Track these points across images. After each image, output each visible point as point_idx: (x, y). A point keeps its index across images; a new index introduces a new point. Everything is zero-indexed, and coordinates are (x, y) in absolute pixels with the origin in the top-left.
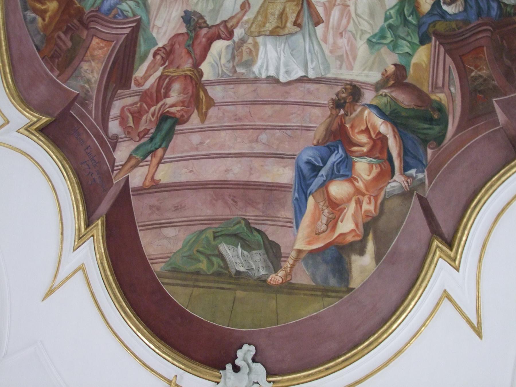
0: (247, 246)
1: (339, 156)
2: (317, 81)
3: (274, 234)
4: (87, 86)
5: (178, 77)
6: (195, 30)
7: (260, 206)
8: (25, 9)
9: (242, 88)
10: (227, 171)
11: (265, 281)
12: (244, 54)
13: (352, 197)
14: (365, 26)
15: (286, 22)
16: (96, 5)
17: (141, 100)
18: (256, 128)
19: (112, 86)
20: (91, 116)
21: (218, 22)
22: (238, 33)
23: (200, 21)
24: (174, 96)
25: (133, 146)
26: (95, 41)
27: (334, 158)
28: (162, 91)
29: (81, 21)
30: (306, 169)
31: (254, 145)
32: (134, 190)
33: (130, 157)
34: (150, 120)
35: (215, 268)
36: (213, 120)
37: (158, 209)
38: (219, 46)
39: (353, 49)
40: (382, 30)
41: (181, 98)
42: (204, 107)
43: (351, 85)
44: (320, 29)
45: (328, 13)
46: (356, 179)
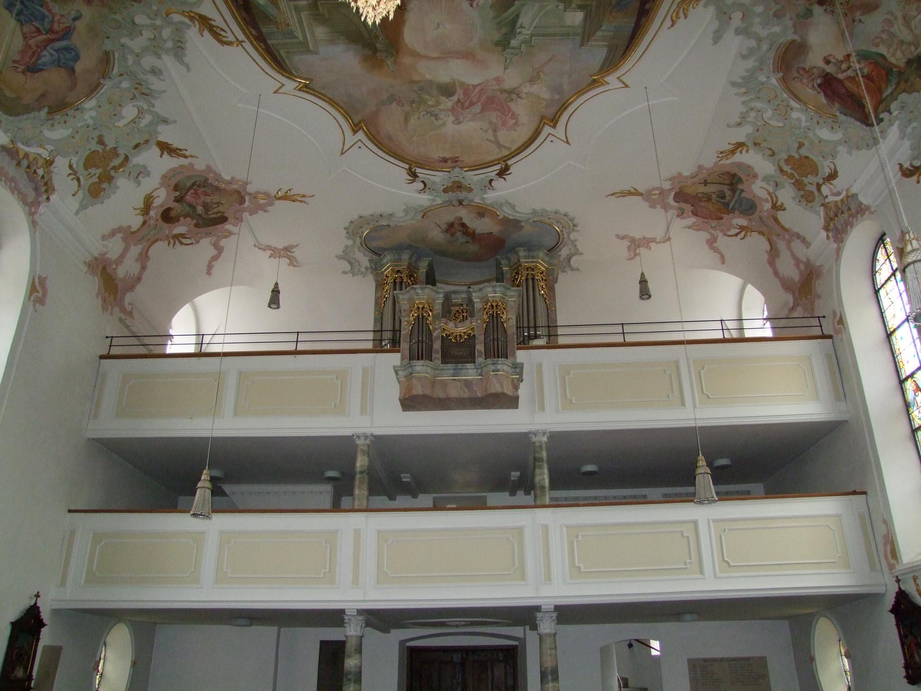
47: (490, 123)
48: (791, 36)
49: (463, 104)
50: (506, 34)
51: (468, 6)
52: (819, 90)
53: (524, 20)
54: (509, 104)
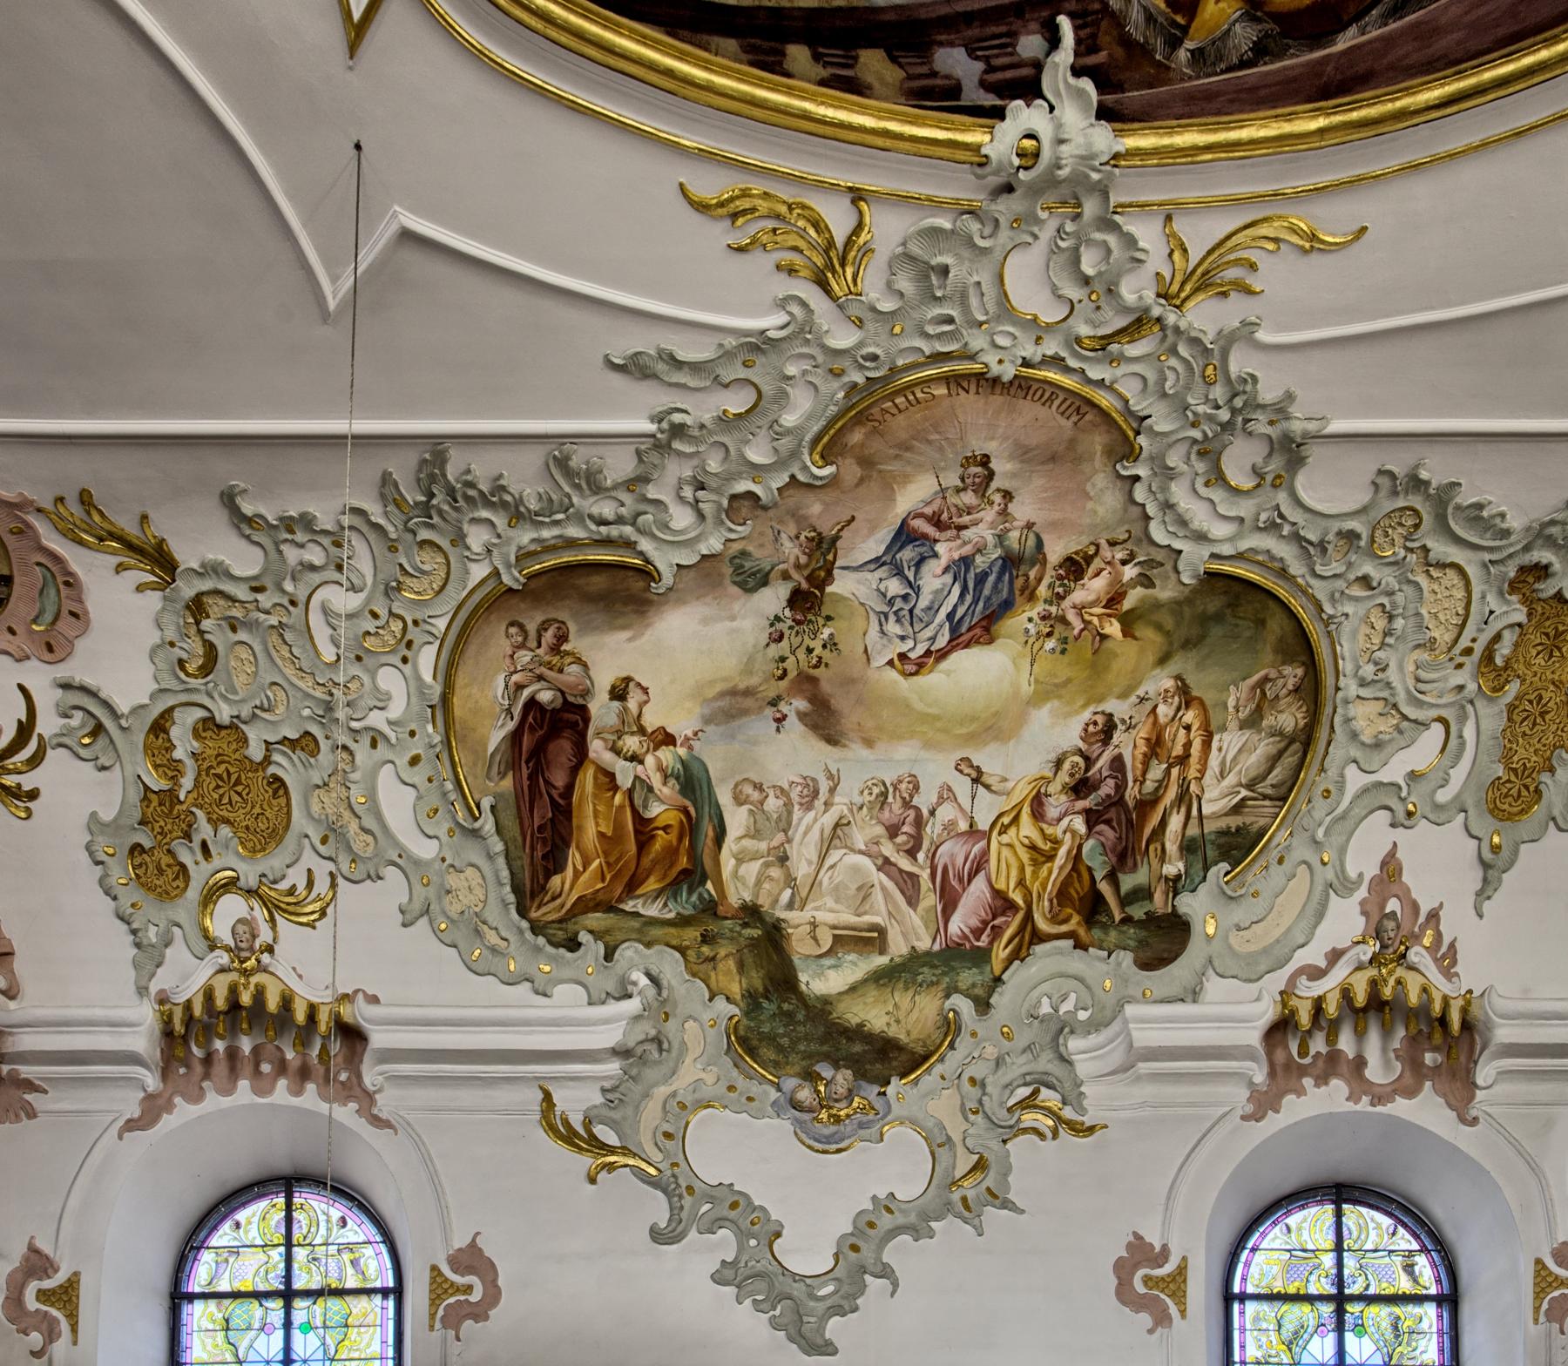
48: (665, 561)
52: (517, 711)
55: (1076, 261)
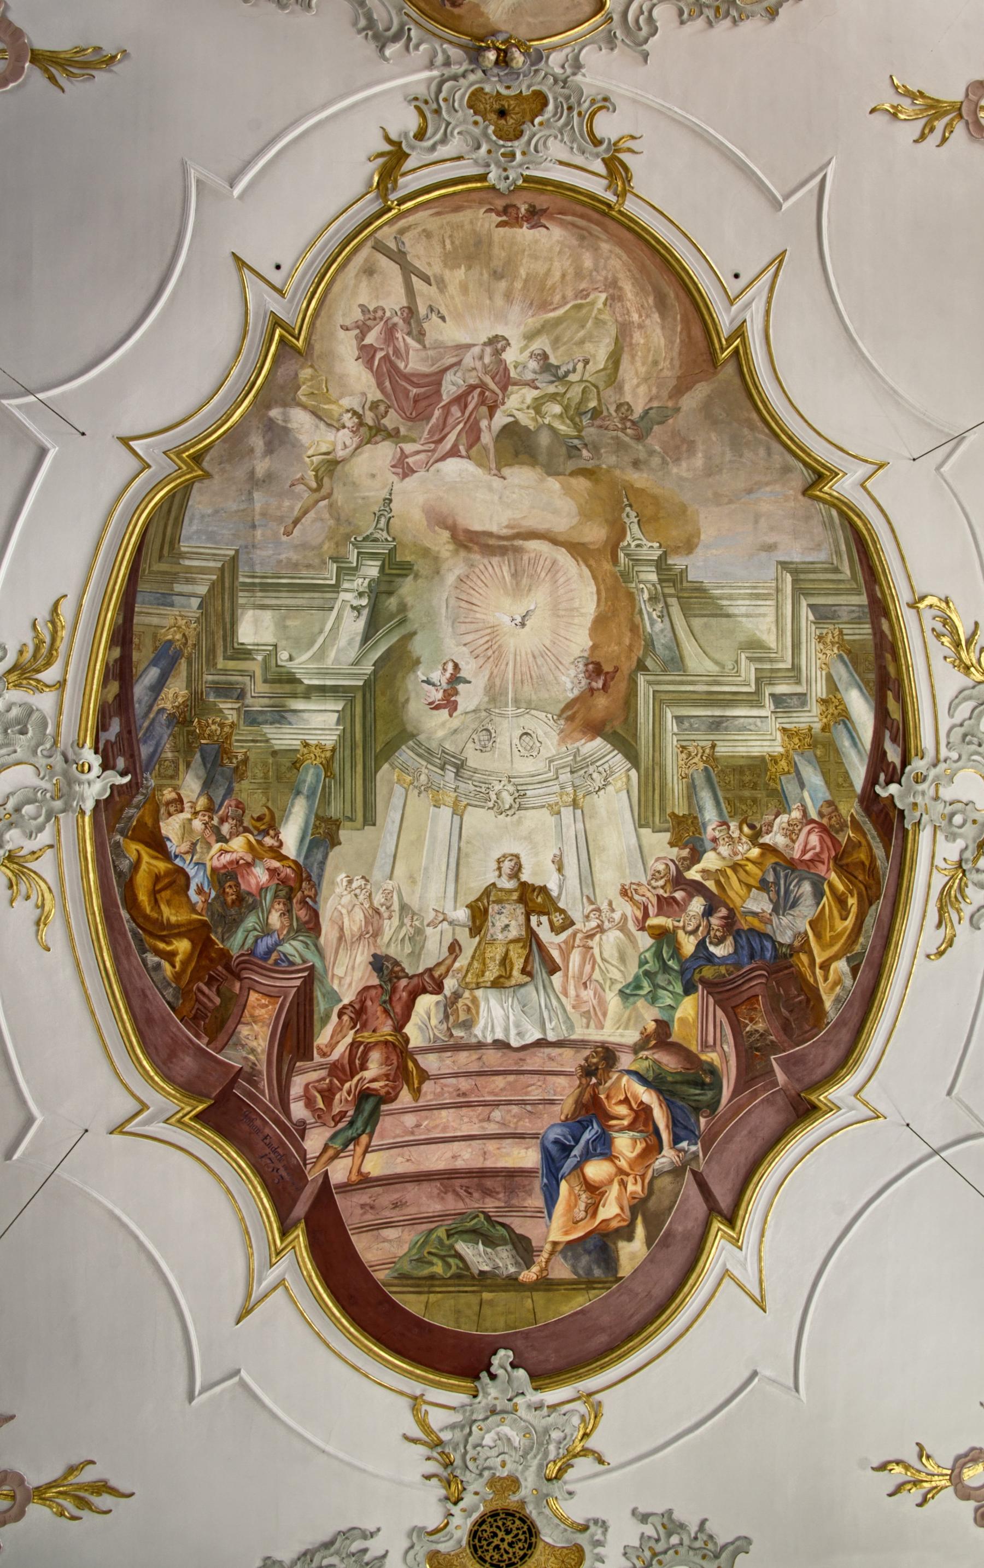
0: (490, 1242)
1: (593, 1132)
2: (559, 1044)
3: (521, 1226)
4: (252, 1057)
5: (376, 1044)
6: (390, 980)
7: (501, 1195)
8: (143, 950)
9: (463, 1056)
10: (454, 1157)
11: (516, 1279)
12: (460, 1012)
13: (613, 1179)
14: (615, 974)
15: (511, 970)
16: (246, 947)
17: (329, 1075)
18: (485, 1104)
19: (287, 1058)
20: (264, 1095)
21: (421, 970)
22: (450, 984)
23: (396, 969)
24: (375, 1067)
25: (327, 1133)
26: (253, 996)
27: (587, 1135)
28: (357, 1062)
29: (227, 967)
30: (554, 1149)
31: (485, 1124)
32: (337, 1187)
33: (326, 1148)
34: (346, 1100)
35: (454, 1269)
36: (430, 1097)
37: (372, 1207)
38: (425, 1002)
39: (602, 1003)
40: (637, 978)
41: (384, 1069)
42: (416, 1082)
43: (603, 1047)
44: (557, 979)
45: (566, 956)
46: (617, 1158)
47: (420, 336)
49: (482, 402)
50: (390, 593)
51: (462, 664)
53: (354, 626)
54: (379, 396)
55: (29, 802)
